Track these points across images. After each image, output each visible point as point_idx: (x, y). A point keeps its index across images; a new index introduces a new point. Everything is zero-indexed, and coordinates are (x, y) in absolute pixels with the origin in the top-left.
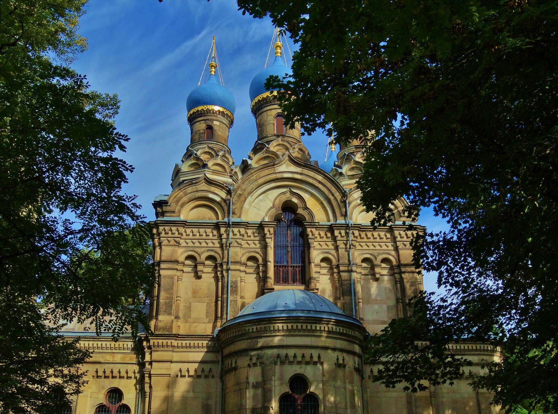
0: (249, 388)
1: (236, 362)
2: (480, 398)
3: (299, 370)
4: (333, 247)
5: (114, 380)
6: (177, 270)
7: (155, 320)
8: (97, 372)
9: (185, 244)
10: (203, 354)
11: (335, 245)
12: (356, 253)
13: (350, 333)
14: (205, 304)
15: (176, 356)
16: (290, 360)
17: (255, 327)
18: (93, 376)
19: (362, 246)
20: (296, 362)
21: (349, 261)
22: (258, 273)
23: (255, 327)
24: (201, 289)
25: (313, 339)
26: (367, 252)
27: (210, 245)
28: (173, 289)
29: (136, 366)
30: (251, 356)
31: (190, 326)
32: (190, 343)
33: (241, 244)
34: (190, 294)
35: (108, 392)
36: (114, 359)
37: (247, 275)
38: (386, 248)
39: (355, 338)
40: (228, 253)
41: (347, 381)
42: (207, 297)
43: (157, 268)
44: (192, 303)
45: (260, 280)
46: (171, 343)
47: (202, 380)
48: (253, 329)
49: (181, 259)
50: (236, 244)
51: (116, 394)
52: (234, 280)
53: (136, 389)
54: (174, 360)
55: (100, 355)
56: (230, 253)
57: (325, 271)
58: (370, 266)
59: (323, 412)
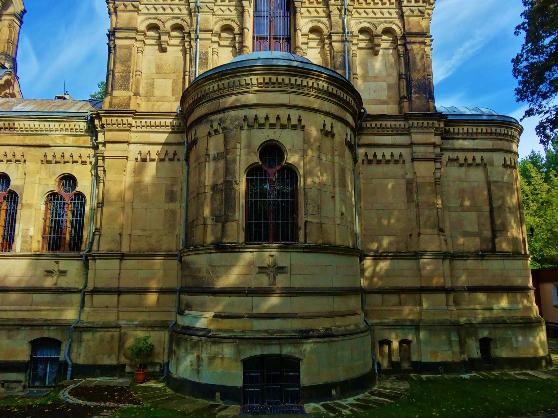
0: (209, 162)
1: (195, 133)
2: (492, 187)
3: (273, 135)
4: (324, 15)
5: (66, 165)
6: (136, 40)
7: (109, 97)
8: (45, 156)
9: (146, 11)
10: (166, 135)
11: (327, 11)
12: (353, 22)
13: (342, 96)
14: (171, 81)
15: (134, 137)
16: (260, 123)
17: (216, 85)
18: (42, 161)
19: (359, 14)
20: (267, 126)
21: (344, 29)
22: (234, 46)
23: (216, 85)
24: (166, 64)
25: (292, 96)
26: (366, 20)
27: (177, 11)
28: (130, 61)
29: (91, 149)
30: (212, 122)
31: (153, 105)
32: (151, 122)
33: (213, 10)
34: (154, 70)
35: (61, 179)
36: (65, 142)
37: (221, 49)
38: (389, 16)
39: (348, 104)
40: (197, 20)
41: (336, 153)
42: (174, 73)
43: (113, 38)
44: (155, 80)
45: (236, 53)
46: (127, 121)
47: (167, 164)
48: (213, 87)
49: (142, 27)
50: (206, 9)
51: (70, 181)
52: (203, 51)
53: (92, 175)
54: (132, 141)
55: (49, 137)
56: (199, 20)
57: (313, 44)
58: (368, 38)
59: (303, 188)
